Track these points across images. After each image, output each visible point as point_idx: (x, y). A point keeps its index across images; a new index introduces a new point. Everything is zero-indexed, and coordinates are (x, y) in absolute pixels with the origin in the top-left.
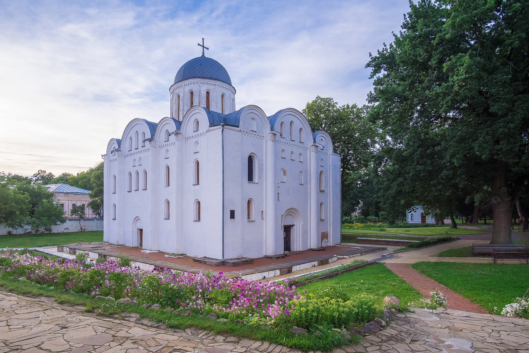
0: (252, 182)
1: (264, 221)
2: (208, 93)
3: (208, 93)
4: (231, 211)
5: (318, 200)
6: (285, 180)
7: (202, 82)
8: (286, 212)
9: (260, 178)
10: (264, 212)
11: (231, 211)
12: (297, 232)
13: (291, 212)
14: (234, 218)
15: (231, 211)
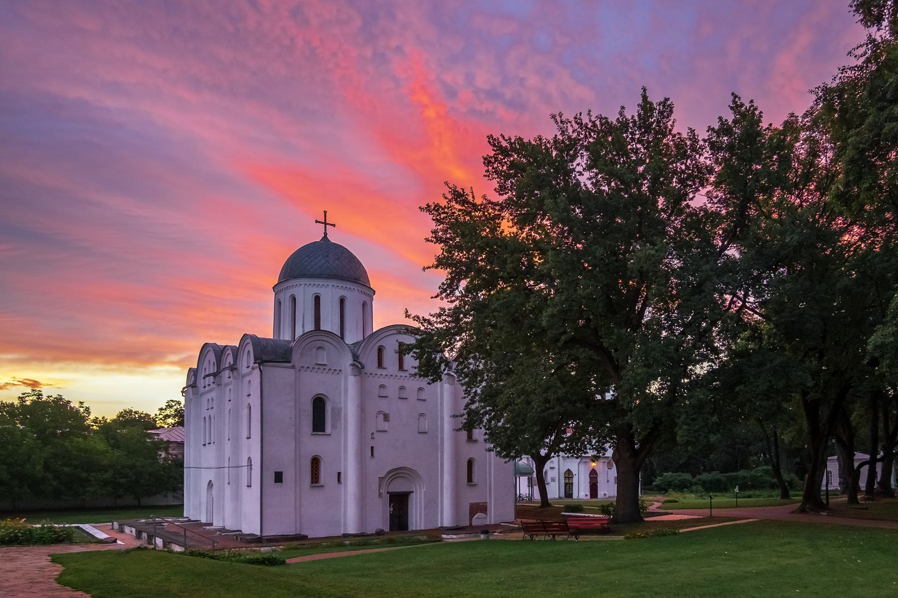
0: (323, 433)
1: (343, 485)
2: (317, 299)
3: (317, 299)
4: (275, 472)
5: (456, 455)
6: (387, 428)
7: (308, 283)
8: (389, 472)
9: (334, 426)
10: (342, 475)
11: (275, 472)
12: (416, 502)
13: (397, 473)
14: (282, 482)
15: (276, 473)
